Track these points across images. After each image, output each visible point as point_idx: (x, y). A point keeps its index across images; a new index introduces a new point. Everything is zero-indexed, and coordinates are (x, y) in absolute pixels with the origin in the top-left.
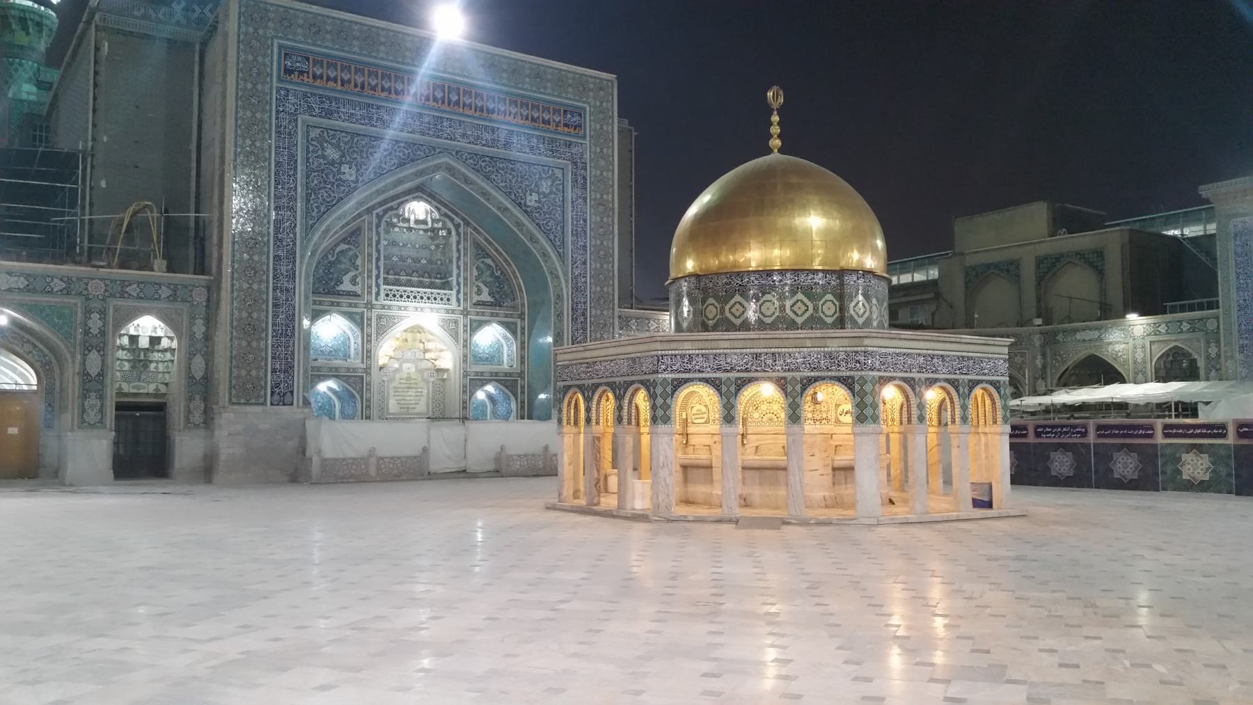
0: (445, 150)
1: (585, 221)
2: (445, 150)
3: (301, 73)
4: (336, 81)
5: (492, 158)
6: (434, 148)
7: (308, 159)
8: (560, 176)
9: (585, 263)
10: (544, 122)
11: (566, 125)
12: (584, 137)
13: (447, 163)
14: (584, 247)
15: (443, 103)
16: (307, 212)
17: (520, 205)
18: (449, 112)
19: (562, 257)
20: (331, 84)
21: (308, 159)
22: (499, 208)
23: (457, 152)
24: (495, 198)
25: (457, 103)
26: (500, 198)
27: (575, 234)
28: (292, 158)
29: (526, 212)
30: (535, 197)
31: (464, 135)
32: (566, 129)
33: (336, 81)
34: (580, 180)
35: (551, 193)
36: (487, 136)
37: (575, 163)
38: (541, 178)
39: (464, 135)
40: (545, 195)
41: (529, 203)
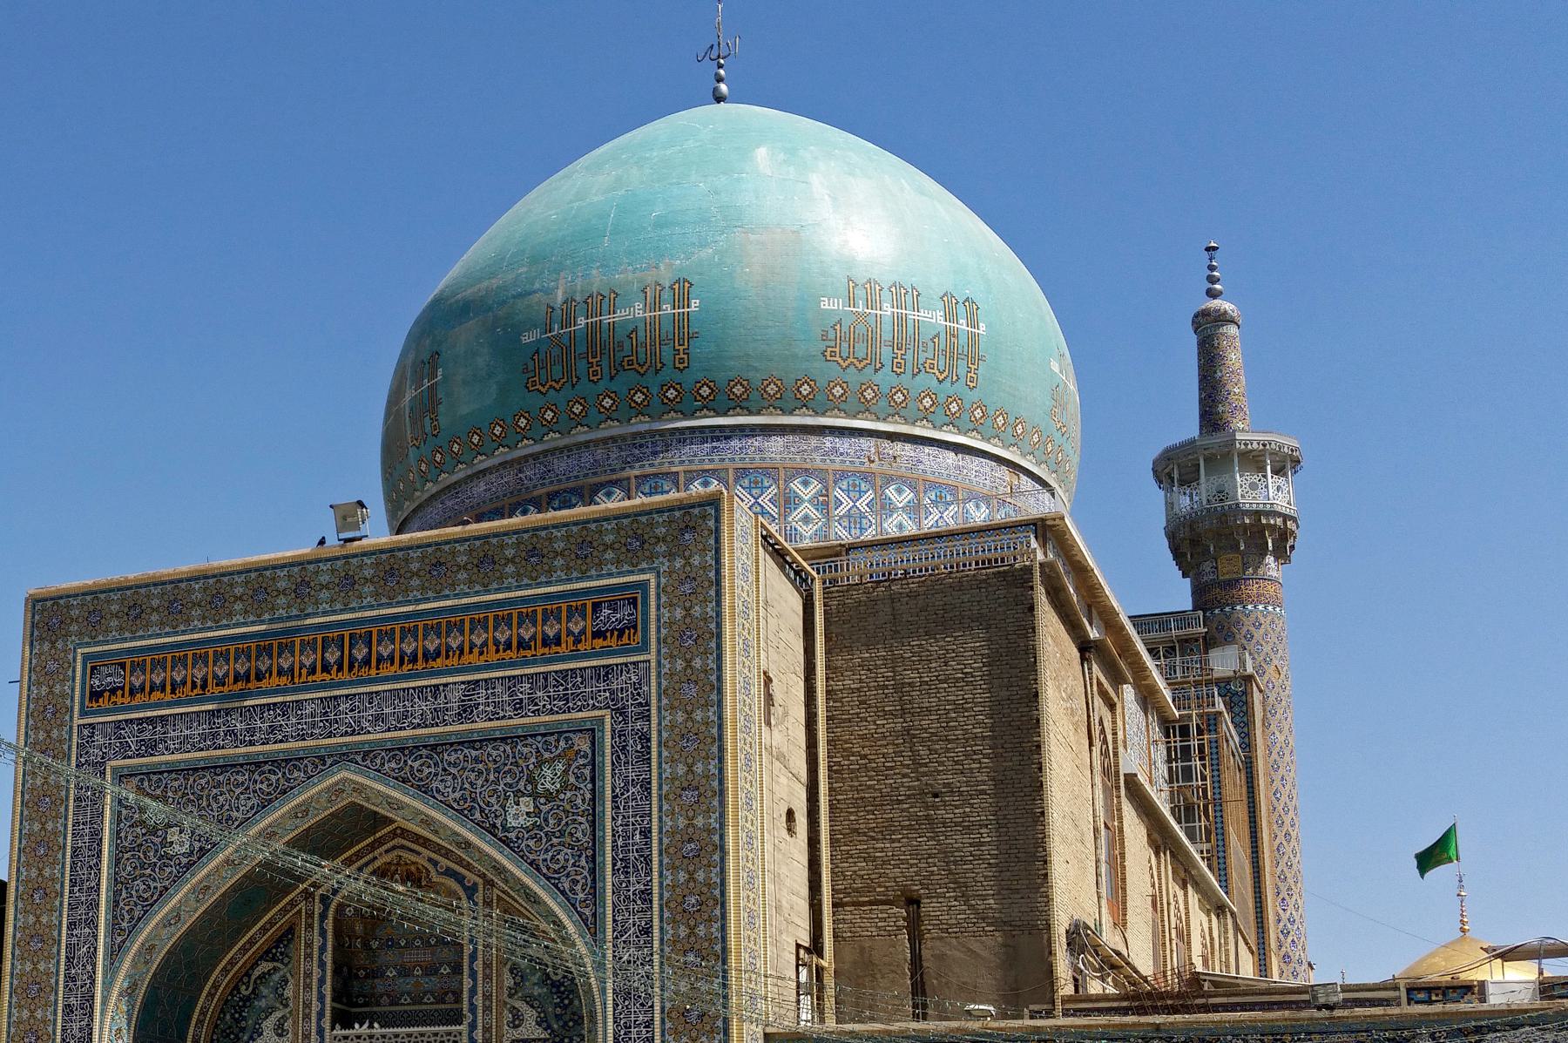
0: (343, 757)
1: (646, 833)
2: (343, 757)
3: (113, 691)
4: (163, 690)
5: (434, 747)
6: (322, 759)
7: (118, 833)
8: (585, 747)
9: (647, 931)
10: (545, 643)
11: (598, 634)
12: (644, 648)
13: (344, 780)
14: (646, 896)
15: (340, 669)
16: (114, 927)
17: (492, 829)
18: (351, 684)
19: (592, 925)
20: (157, 695)
21: (118, 833)
22: (458, 845)
23: (366, 754)
24: (445, 827)
25: (367, 662)
26: (451, 824)
27: (623, 867)
28: (96, 837)
29: (506, 842)
30: (526, 804)
31: (378, 718)
32: (599, 642)
33: (163, 690)
34: (633, 746)
35: (566, 786)
36: (422, 706)
37: (621, 711)
38: (540, 764)
39: (378, 718)
40: (549, 796)
41: (512, 822)
